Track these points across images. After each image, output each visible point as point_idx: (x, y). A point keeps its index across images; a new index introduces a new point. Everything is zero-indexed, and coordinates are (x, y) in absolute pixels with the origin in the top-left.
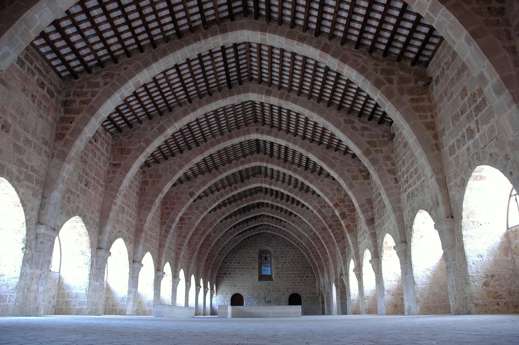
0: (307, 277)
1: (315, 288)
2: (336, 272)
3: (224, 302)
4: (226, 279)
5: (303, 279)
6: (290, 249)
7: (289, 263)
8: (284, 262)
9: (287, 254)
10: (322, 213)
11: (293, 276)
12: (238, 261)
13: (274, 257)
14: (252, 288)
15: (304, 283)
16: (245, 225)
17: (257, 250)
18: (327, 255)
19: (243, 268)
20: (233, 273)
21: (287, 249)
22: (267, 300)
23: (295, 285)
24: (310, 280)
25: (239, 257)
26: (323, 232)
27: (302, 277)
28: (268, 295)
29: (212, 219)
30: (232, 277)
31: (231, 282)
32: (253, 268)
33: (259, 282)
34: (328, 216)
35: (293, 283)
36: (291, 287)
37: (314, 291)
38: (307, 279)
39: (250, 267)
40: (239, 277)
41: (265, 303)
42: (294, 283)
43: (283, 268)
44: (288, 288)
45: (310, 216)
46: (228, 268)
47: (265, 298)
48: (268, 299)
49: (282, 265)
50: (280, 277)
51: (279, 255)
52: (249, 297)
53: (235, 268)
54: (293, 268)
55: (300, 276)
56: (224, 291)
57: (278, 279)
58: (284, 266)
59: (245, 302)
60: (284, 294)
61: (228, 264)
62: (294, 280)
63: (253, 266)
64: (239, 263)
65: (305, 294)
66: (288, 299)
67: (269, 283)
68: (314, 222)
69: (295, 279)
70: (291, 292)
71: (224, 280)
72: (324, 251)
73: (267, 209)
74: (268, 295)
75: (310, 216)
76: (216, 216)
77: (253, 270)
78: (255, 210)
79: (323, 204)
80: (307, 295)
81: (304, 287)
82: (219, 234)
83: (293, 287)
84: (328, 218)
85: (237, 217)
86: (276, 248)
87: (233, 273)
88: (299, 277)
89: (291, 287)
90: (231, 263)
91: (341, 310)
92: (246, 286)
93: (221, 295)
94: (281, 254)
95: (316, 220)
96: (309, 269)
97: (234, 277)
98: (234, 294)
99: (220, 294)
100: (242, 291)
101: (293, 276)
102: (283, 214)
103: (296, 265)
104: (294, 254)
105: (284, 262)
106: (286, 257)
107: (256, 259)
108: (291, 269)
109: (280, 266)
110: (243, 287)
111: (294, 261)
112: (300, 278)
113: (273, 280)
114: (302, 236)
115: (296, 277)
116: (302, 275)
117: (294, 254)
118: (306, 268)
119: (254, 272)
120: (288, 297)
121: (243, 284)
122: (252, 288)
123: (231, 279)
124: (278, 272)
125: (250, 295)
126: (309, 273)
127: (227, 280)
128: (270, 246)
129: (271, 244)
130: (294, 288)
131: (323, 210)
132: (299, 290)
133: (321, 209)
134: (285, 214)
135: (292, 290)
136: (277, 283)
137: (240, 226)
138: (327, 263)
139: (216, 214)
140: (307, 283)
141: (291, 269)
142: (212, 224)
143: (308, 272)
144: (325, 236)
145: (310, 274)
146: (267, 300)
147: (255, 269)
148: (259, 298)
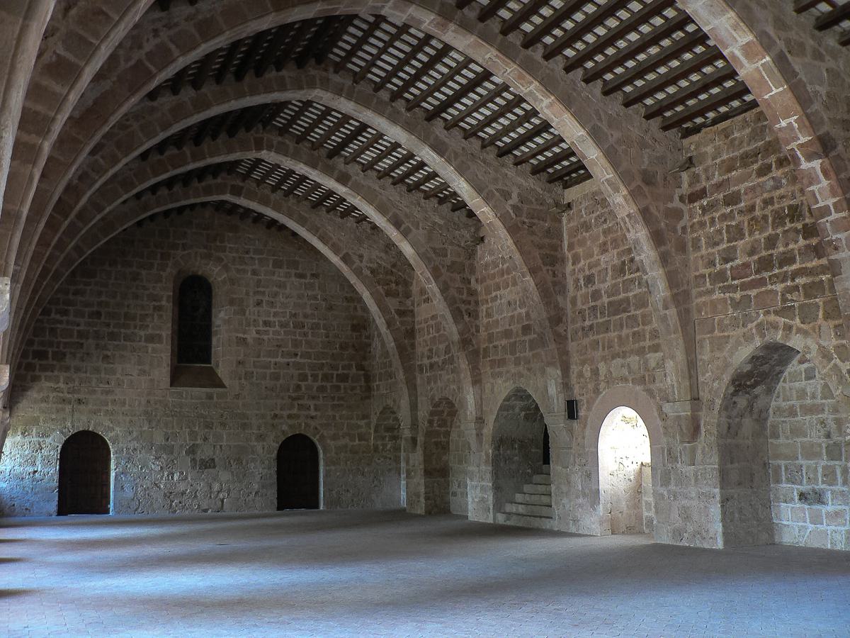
0: (343, 378)
1: (365, 417)
2: (692, 366)
3: (34, 464)
4: (43, 375)
5: (329, 385)
6: (288, 275)
7: (281, 326)
8: (266, 323)
9: (276, 294)
10: (795, 74)
11: (296, 373)
12: (95, 309)
13: (232, 302)
14: (146, 413)
15: (333, 398)
16: (187, 150)
17: (170, 271)
18: (560, 299)
19: (113, 336)
20: (74, 355)
21: (275, 278)
22: (199, 456)
23: (301, 407)
24: (353, 389)
25: (100, 294)
26: (646, 189)
27: (326, 377)
28: (205, 439)
29: (148, 47)
30: (67, 369)
31: (61, 385)
32: (151, 339)
33: (173, 390)
34: (816, 93)
35: (294, 399)
36: (285, 413)
37: (363, 430)
38: (342, 385)
39: (142, 333)
40: (97, 370)
41: (193, 467)
42: (298, 398)
43: (260, 342)
44: (276, 416)
45: (597, 113)
46: (52, 330)
47: (192, 451)
48: (205, 453)
49: (258, 332)
50: (248, 375)
51: (247, 294)
52: (131, 445)
53: (81, 334)
54: (296, 344)
55: (320, 373)
56: (35, 421)
57: (243, 381)
58: (266, 337)
59: (117, 465)
60: (261, 437)
61: (53, 315)
62: (299, 387)
63: (150, 331)
64: (98, 314)
65: (335, 437)
66: (274, 455)
67: (210, 397)
68: (612, 140)
69: (303, 384)
70: (286, 429)
71: (35, 379)
72: (549, 278)
73: (336, 78)
74: (205, 439)
75: (597, 113)
76: (164, 36)
77: (150, 346)
78: (284, 73)
79: (792, 35)
80: (341, 442)
81: (330, 413)
82: (115, 161)
83: (295, 411)
84: (816, 106)
85: (204, 90)
86: (238, 271)
87: (74, 355)
88: (315, 377)
89: (285, 413)
90: (65, 313)
91: (718, 528)
92: (124, 404)
93: (19, 438)
94: (256, 293)
95: (617, 134)
96: (351, 351)
97: (78, 370)
98: (72, 432)
99: (15, 431)
100: (107, 423)
101: (296, 373)
102: (403, 110)
103: (305, 334)
104: (300, 297)
105: (266, 323)
106: (272, 304)
107: (164, 303)
108: (290, 348)
109: (251, 335)
110: (110, 407)
111: (301, 319)
112: (319, 383)
113: (223, 386)
114: (407, 224)
115: (303, 377)
116: (326, 370)
117: (300, 297)
118: (341, 348)
119: (153, 349)
120: (277, 446)
121: (110, 397)
122: (146, 413)
123: (62, 376)
124: (240, 358)
125: (136, 439)
126: (349, 367)
127: (48, 379)
128: (220, 260)
129: (222, 255)
130: (297, 417)
131: (796, 63)
132: (313, 423)
133: (789, 56)
134: (409, 110)
135: (291, 422)
136: (237, 396)
137: (167, 153)
138: (560, 329)
139: (168, 26)
140: (342, 399)
141: (290, 348)
142: (140, 73)
143: (346, 363)
144: (653, 210)
145: (354, 370)
146: (199, 456)
147: (160, 341)
148: (169, 450)
